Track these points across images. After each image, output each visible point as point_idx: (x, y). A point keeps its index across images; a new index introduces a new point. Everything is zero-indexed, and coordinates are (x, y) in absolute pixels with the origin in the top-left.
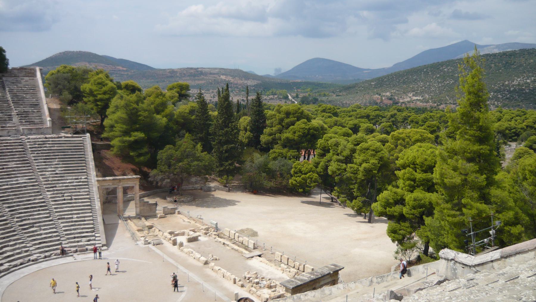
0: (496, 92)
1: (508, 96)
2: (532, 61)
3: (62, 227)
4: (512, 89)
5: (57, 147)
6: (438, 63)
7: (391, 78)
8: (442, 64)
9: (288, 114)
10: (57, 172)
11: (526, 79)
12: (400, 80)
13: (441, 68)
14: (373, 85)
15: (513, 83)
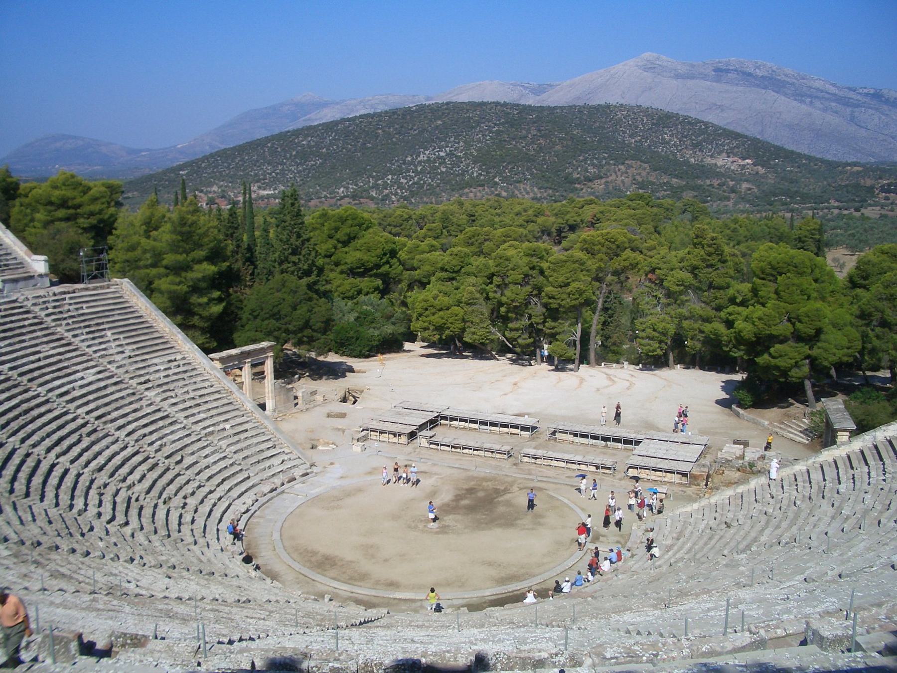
0: (394, 175)
1: (416, 179)
2: (440, 122)
3: (224, 447)
4: (419, 168)
5: (88, 308)
6: (289, 132)
7: (214, 162)
8: (297, 133)
9: (343, 220)
10: (127, 354)
11: (438, 151)
12: (230, 164)
13: (296, 141)
14: (182, 175)
15: (419, 159)
